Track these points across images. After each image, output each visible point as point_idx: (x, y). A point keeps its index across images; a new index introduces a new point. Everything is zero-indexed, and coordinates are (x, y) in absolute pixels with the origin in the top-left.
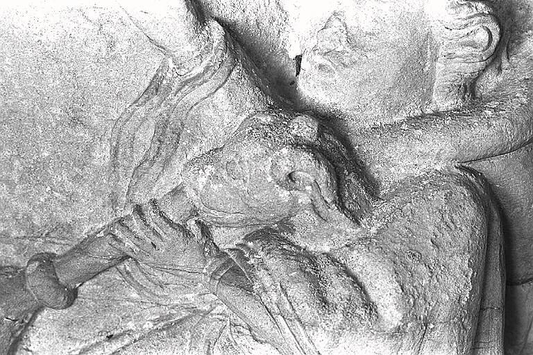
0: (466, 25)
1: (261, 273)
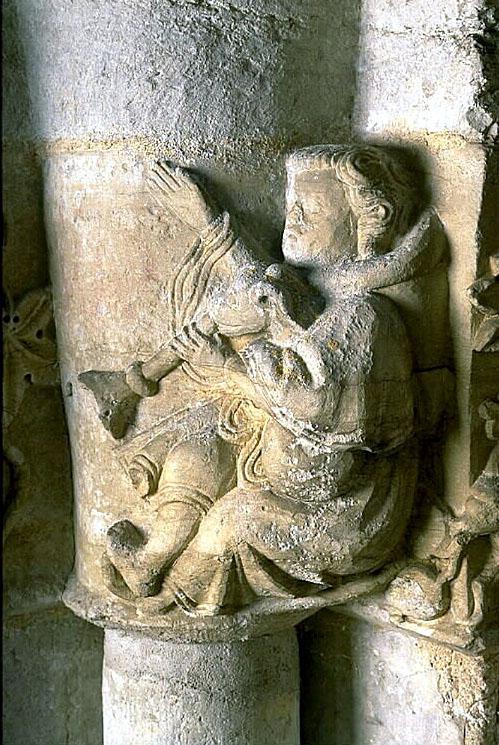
0: (370, 205)
1: (251, 362)
